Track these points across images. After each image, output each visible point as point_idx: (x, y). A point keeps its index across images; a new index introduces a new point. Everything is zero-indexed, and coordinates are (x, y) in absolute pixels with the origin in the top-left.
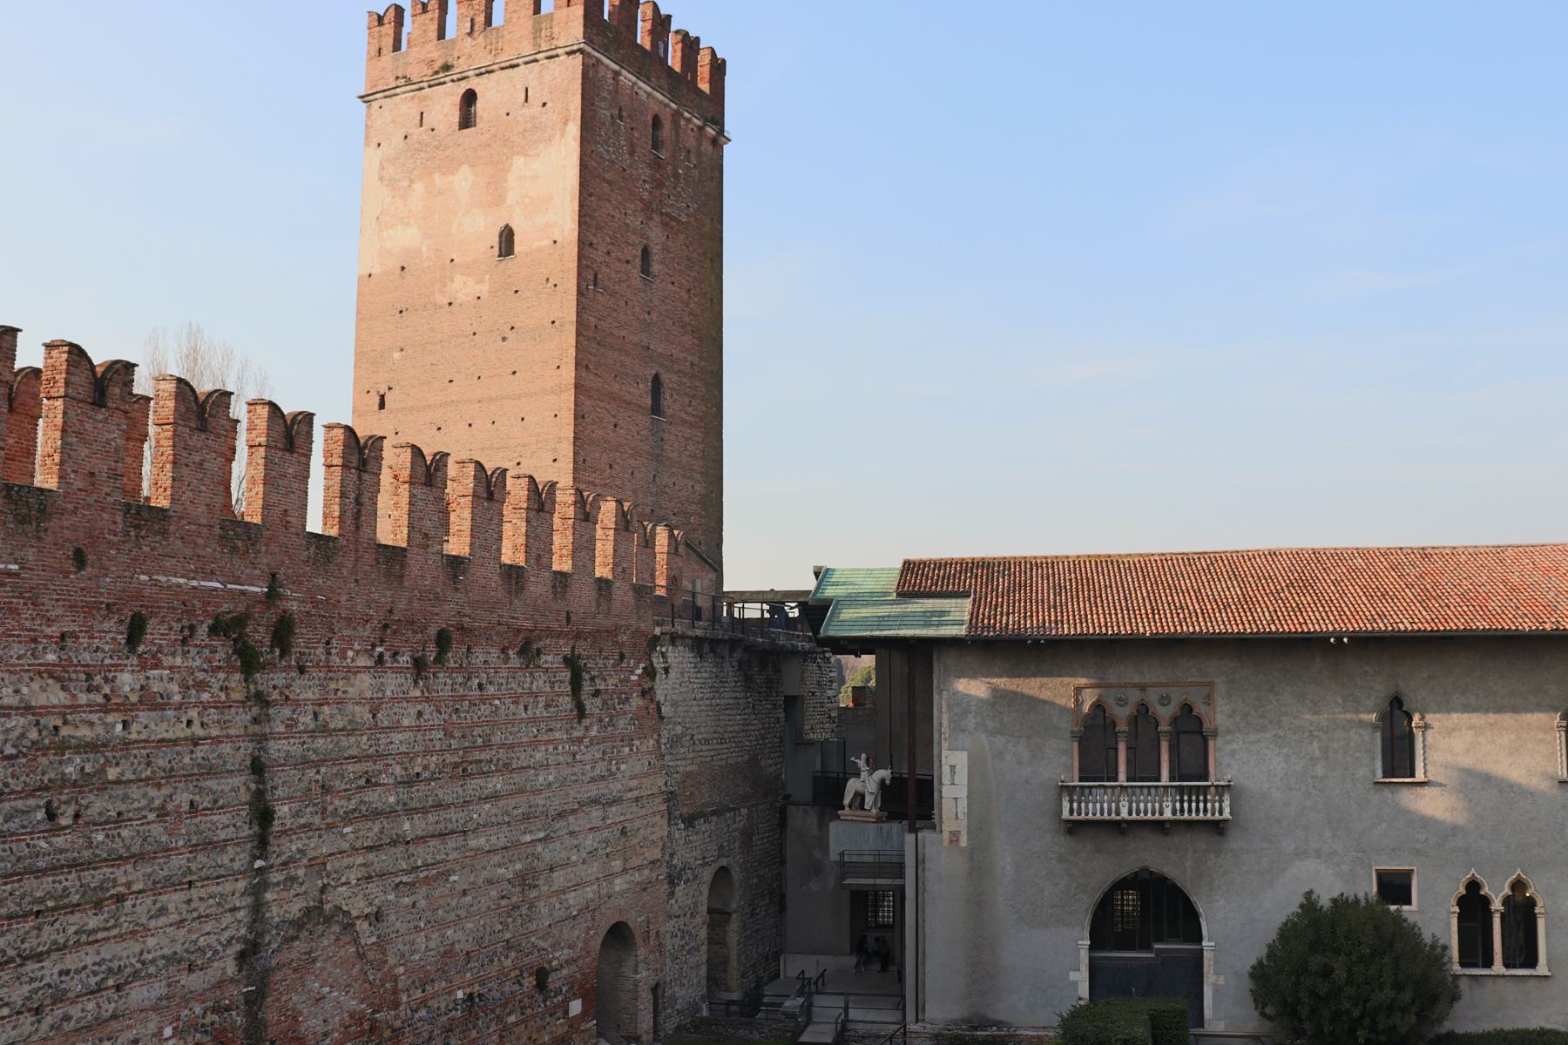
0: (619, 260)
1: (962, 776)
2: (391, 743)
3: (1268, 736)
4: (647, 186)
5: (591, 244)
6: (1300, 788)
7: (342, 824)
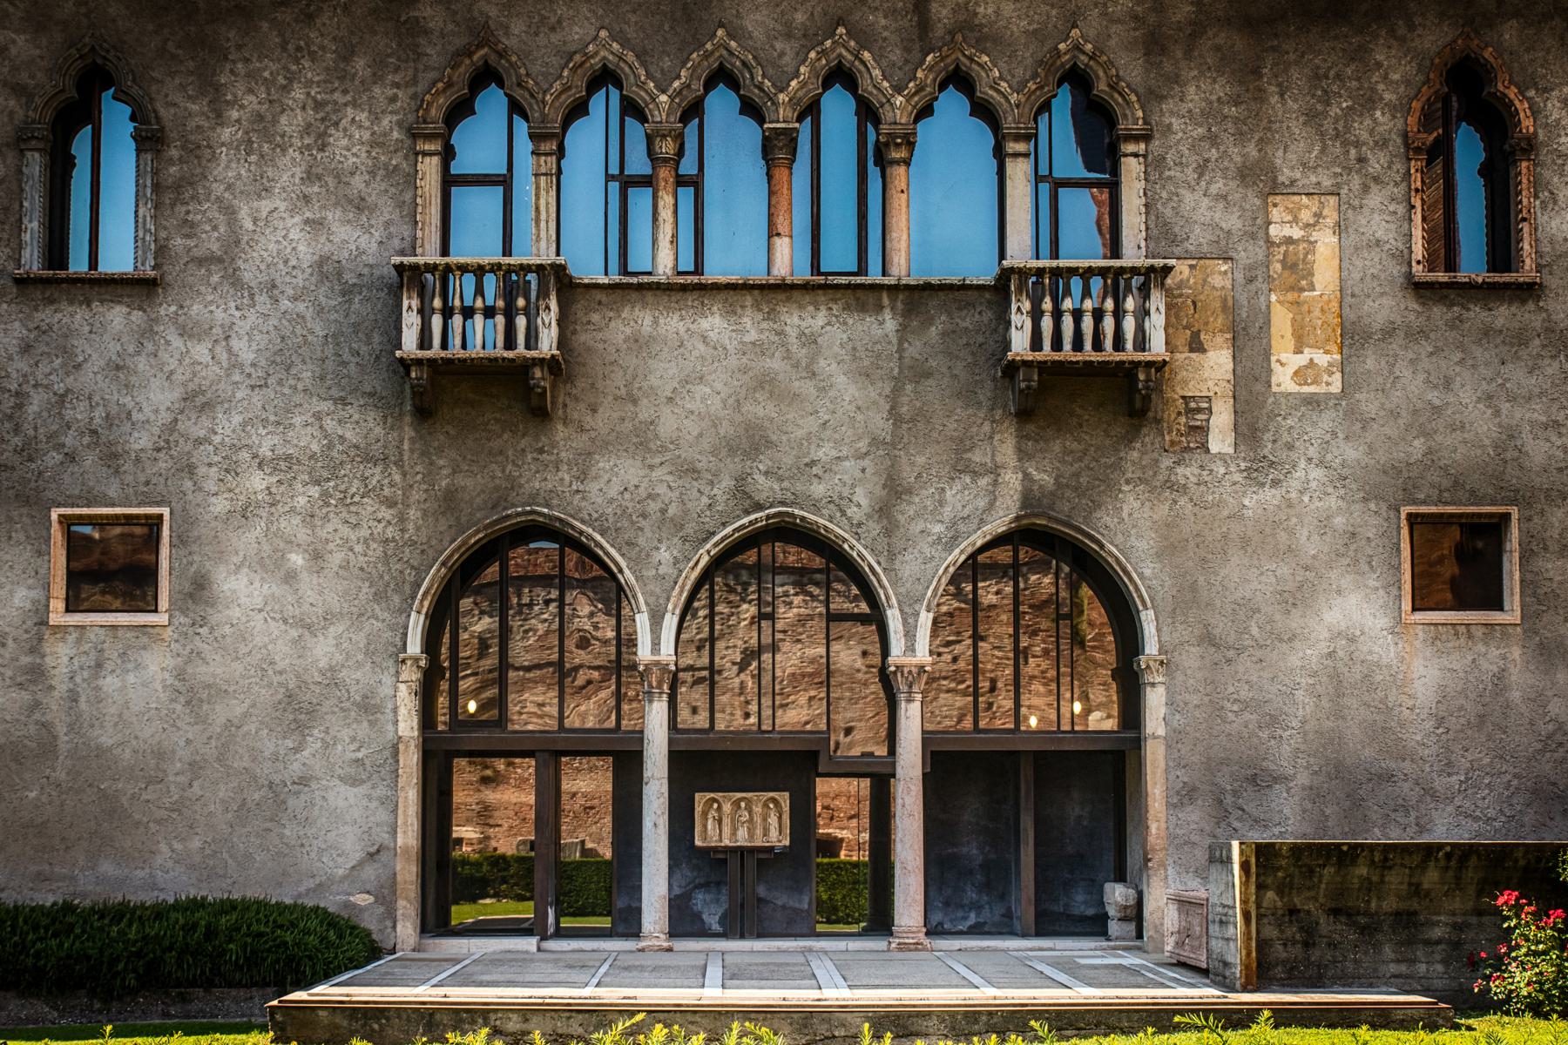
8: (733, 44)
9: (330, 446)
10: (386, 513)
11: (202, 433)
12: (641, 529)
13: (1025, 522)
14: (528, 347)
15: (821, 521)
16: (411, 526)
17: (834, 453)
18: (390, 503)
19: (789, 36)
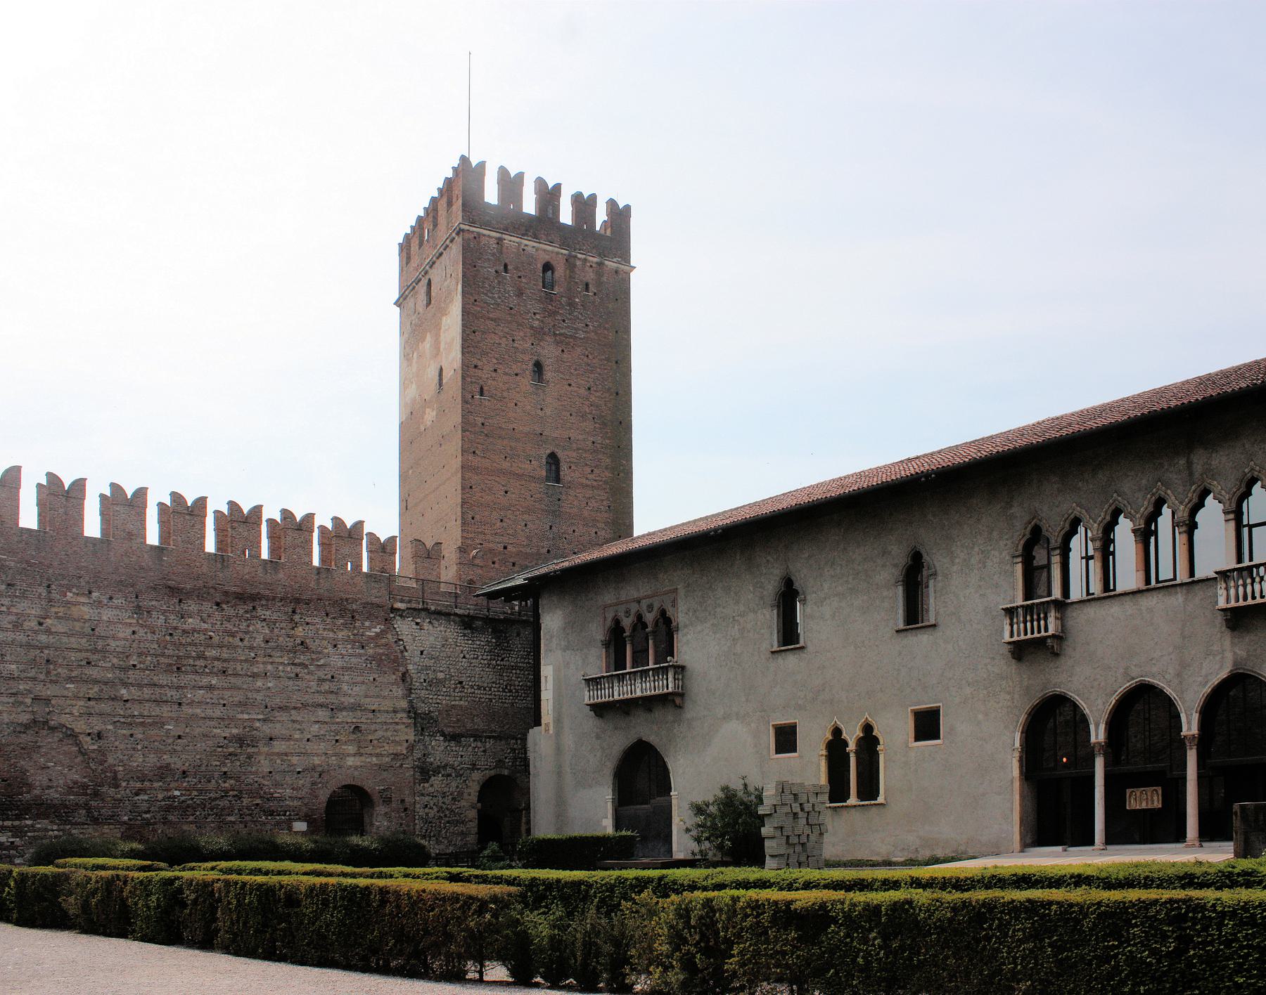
0: (506, 374)
1: (550, 679)
2: (108, 645)
3: (708, 625)
4: (538, 316)
5: (476, 367)
6: (727, 664)
7: (65, 682)
8: (1120, 498)
9: (989, 675)
10: (1008, 697)
11: (951, 676)
12: (1091, 693)
13: (1235, 672)
14: (1045, 632)
15: (1155, 681)
16: (1015, 701)
17: (1160, 654)
18: (1009, 693)
19: (1140, 490)
